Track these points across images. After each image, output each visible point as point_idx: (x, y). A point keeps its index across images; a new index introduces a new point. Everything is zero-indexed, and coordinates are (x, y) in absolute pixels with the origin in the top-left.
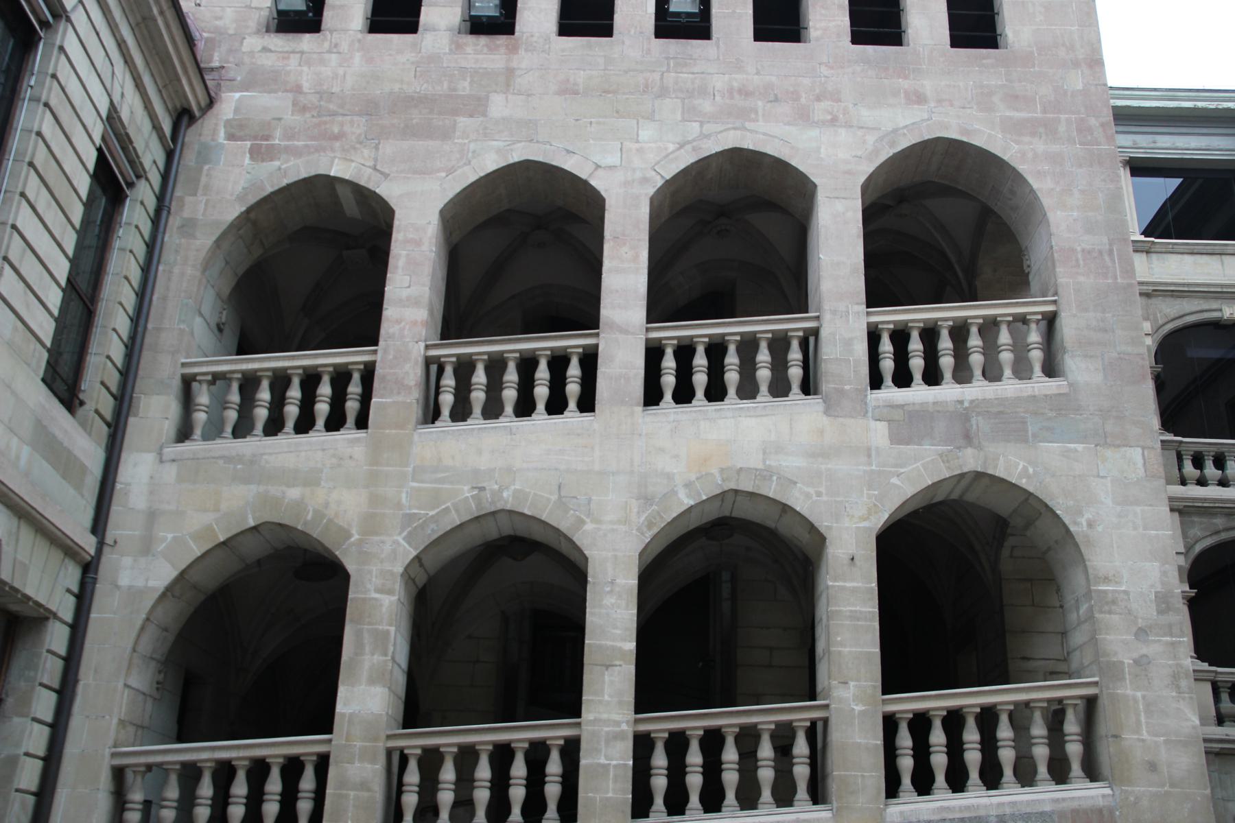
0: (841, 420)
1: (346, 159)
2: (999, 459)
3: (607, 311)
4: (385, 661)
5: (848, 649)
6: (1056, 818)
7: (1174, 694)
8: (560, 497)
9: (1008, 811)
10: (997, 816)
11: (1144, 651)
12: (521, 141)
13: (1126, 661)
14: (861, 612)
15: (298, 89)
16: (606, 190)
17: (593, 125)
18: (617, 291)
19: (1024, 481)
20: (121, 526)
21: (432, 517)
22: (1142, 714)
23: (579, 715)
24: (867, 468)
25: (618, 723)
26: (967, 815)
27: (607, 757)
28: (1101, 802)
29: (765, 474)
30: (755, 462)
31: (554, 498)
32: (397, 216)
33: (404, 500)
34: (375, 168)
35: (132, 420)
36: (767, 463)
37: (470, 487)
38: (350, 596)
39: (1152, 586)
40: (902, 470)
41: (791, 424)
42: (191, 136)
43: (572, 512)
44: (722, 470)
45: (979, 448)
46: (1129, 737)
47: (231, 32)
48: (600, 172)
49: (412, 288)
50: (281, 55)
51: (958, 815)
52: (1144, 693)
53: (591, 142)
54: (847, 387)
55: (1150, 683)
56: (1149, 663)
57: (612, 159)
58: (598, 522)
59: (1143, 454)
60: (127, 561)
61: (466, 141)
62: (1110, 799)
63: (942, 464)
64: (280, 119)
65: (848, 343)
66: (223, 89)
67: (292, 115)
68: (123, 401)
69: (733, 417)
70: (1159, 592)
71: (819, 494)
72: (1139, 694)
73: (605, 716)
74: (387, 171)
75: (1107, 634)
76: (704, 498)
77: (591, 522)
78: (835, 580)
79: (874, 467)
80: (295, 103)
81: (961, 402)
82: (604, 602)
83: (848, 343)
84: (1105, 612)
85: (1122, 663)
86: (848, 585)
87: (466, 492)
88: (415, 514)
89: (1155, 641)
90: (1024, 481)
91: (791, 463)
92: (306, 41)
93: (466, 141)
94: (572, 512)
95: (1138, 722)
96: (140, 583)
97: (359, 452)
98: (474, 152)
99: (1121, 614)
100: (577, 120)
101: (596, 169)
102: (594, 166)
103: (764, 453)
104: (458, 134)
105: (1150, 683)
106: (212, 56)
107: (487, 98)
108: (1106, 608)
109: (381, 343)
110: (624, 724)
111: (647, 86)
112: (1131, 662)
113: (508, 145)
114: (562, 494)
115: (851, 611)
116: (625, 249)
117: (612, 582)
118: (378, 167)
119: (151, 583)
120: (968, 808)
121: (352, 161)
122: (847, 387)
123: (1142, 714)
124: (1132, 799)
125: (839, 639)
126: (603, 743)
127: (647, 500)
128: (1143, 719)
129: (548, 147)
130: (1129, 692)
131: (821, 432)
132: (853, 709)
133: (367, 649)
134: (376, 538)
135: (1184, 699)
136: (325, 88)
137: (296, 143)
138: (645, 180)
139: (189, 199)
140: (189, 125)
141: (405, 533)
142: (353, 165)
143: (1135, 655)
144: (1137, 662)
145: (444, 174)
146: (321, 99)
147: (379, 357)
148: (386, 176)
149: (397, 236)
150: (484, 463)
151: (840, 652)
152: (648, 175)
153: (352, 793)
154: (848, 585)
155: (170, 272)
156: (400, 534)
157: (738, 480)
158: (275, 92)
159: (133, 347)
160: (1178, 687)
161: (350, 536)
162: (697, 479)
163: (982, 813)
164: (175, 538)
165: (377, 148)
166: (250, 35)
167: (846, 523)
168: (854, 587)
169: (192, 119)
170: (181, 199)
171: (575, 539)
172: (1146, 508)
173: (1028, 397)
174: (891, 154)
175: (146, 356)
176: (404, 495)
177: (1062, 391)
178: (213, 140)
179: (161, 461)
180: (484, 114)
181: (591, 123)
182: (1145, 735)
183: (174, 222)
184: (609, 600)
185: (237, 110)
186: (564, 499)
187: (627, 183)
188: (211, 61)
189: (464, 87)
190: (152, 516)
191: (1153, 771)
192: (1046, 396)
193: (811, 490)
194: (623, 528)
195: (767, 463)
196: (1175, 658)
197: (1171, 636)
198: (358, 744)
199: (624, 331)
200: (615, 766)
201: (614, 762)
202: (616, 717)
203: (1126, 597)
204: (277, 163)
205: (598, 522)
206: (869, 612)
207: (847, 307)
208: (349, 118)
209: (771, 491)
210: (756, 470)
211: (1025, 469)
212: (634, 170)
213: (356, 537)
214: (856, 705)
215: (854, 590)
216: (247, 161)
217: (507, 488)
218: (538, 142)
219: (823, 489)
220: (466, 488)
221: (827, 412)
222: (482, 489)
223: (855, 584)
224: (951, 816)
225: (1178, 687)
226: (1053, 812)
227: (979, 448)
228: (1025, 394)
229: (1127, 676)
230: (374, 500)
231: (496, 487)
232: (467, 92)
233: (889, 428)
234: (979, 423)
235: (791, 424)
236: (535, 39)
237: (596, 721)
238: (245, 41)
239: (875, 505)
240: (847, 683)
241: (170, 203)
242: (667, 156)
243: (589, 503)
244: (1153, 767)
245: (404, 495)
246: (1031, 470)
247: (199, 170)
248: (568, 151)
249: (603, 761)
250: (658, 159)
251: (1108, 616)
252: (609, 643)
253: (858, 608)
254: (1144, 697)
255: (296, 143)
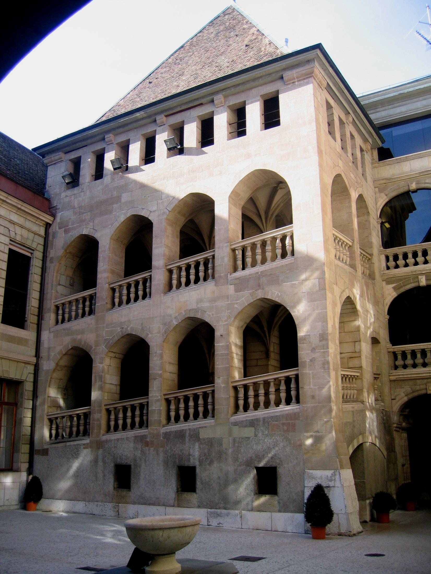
0: (220, 287)
1: (86, 228)
2: (269, 292)
3: (155, 263)
4: (102, 384)
5: (220, 367)
6: (281, 417)
7: (323, 370)
8: (142, 327)
9: (266, 416)
10: (263, 418)
11: (314, 356)
12: (130, 209)
13: (307, 360)
14: (224, 353)
15: (74, 208)
16: (153, 220)
17: (149, 197)
18: (156, 255)
19: (277, 299)
20: (43, 353)
21: (111, 339)
22: (311, 379)
23: (148, 395)
24: (228, 303)
25: (157, 397)
26: (253, 418)
27: (155, 408)
28: (296, 411)
29: (197, 310)
30: (194, 306)
31: (140, 328)
32: (99, 243)
33: (104, 335)
34: (94, 229)
35: (43, 322)
36: (198, 306)
37: (120, 328)
38: (93, 366)
39: (318, 332)
40: (238, 302)
41: (205, 291)
42: (51, 231)
43: (145, 332)
44: (185, 311)
45: (263, 289)
46: (306, 387)
47: (58, 193)
48: (152, 214)
49: (104, 266)
50: (70, 197)
51: (251, 418)
52: (313, 371)
53: (149, 203)
54: (222, 275)
55: (315, 367)
56: (315, 360)
57: (155, 208)
58: (152, 334)
59: (319, 281)
60: (45, 363)
61: (116, 213)
62: (298, 409)
63: (251, 297)
64: (70, 219)
65: (223, 258)
66: (57, 213)
67: (73, 216)
68: (40, 316)
69: (188, 292)
70: (320, 333)
71: (213, 315)
72: (311, 372)
73: (154, 395)
74: (96, 229)
75: (302, 351)
76: (180, 321)
77: (150, 334)
78: (217, 344)
79: (229, 302)
80: (74, 213)
81: (258, 273)
82: (154, 359)
83: (223, 258)
84: (301, 344)
85: (306, 361)
86: (221, 344)
87: (119, 329)
88: (107, 338)
89: (318, 352)
90: (277, 299)
91: (205, 305)
92: (76, 190)
93: (116, 213)
94: (145, 332)
95: (310, 382)
96: (48, 368)
97: (93, 322)
98: (118, 216)
99: (307, 343)
100: (145, 197)
101: (150, 213)
102: (150, 212)
103: (197, 303)
104: (114, 211)
105: (315, 367)
106: (54, 202)
107: (121, 196)
108: (302, 342)
109: (97, 286)
110: (159, 397)
111: (164, 178)
112: (309, 360)
113: (127, 211)
114: (143, 326)
115: (221, 353)
116: (158, 240)
117: (156, 353)
118: (94, 228)
119: (50, 368)
120: (254, 416)
121: (88, 228)
122: (222, 275)
123: (311, 379)
124: (306, 409)
125: (218, 363)
126: (154, 403)
127: (165, 324)
128: (311, 381)
129: (137, 208)
130: (308, 372)
131: (214, 292)
132: (221, 386)
133: (98, 380)
134: (98, 347)
135: (326, 372)
136: (80, 205)
137: (74, 226)
138: (164, 213)
139: (51, 251)
140: (50, 227)
141: (105, 345)
142: (88, 229)
143: (310, 358)
144: (311, 360)
145: (110, 226)
146: (80, 209)
147: (97, 291)
148: (96, 230)
149: (100, 250)
150: (123, 320)
151: (218, 367)
152: (165, 211)
153: (96, 422)
154: (221, 344)
155: (48, 275)
156: (103, 345)
157: (189, 314)
158: (68, 210)
159: (41, 300)
160: (324, 368)
161: (92, 348)
162: (178, 315)
163: (258, 417)
164: (54, 355)
165: (94, 222)
166: (62, 192)
167: (221, 323)
168: (222, 345)
169: (50, 225)
170: (49, 251)
171: (146, 340)
172: (318, 302)
173: (280, 266)
174: (239, 181)
175: (45, 302)
176: (104, 333)
177: (292, 262)
178: (56, 230)
179: (50, 332)
180: (120, 202)
181: (149, 196)
182: (312, 386)
183: (48, 259)
184: (155, 358)
185: (60, 219)
186: (143, 328)
187: (159, 216)
188: (54, 204)
189: (115, 194)
190: (49, 348)
191: (313, 398)
192: (286, 265)
193: (211, 314)
194: (158, 335)
195: (198, 306)
196: (324, 357)
197: (324, 349)
198: (97, 408)
199: (158, 268)
200: (157, 410)
201: (157, 408)
202: (157, 395)
203: (309, 337)
204: (70, 234)
205: (152, 334)
206: (227, 353)
207: (223, 245)
208: (86, 213)
209: (199, 316)
210: (195, 309)
211: (278, 294)
212: (161, 210)
213: (94, 348)
214: (222, 385)
215: (222, 346)
216: (64, 235)
217: (129, 327)
218: (135, 208)
219: (214, 313)
220: (119, 328)
221: (215, 285)
222: (123, 328)
223: (223, 344)
224: (249, 419)
225: (324, 368)
226: (280, 415)
227: (263, 289)
228: (279, 266)
229: (307, 366)
230: (98, 336)
231: (126, 327)
232: (116, 195)
233: (235, 287)
234: (263, 280)
235: (205, 291)
236: (133, 170)
237: (152, 396)
238: (62, 195)
239: (229, 315)
240: (219, 378)
241: (46, 254)
242: (170, 202)
243: (150, 328)
244: (313, 397)
245: (104, 333)
246: (280, 294)
247: (53, 241)
248: (143, 209)
249: (154, 408)
250: (167, 204)
251: (302, 345)
252: (155, 372)
253: (224, 352)
254: (312, 373)
255: (74, 226)
